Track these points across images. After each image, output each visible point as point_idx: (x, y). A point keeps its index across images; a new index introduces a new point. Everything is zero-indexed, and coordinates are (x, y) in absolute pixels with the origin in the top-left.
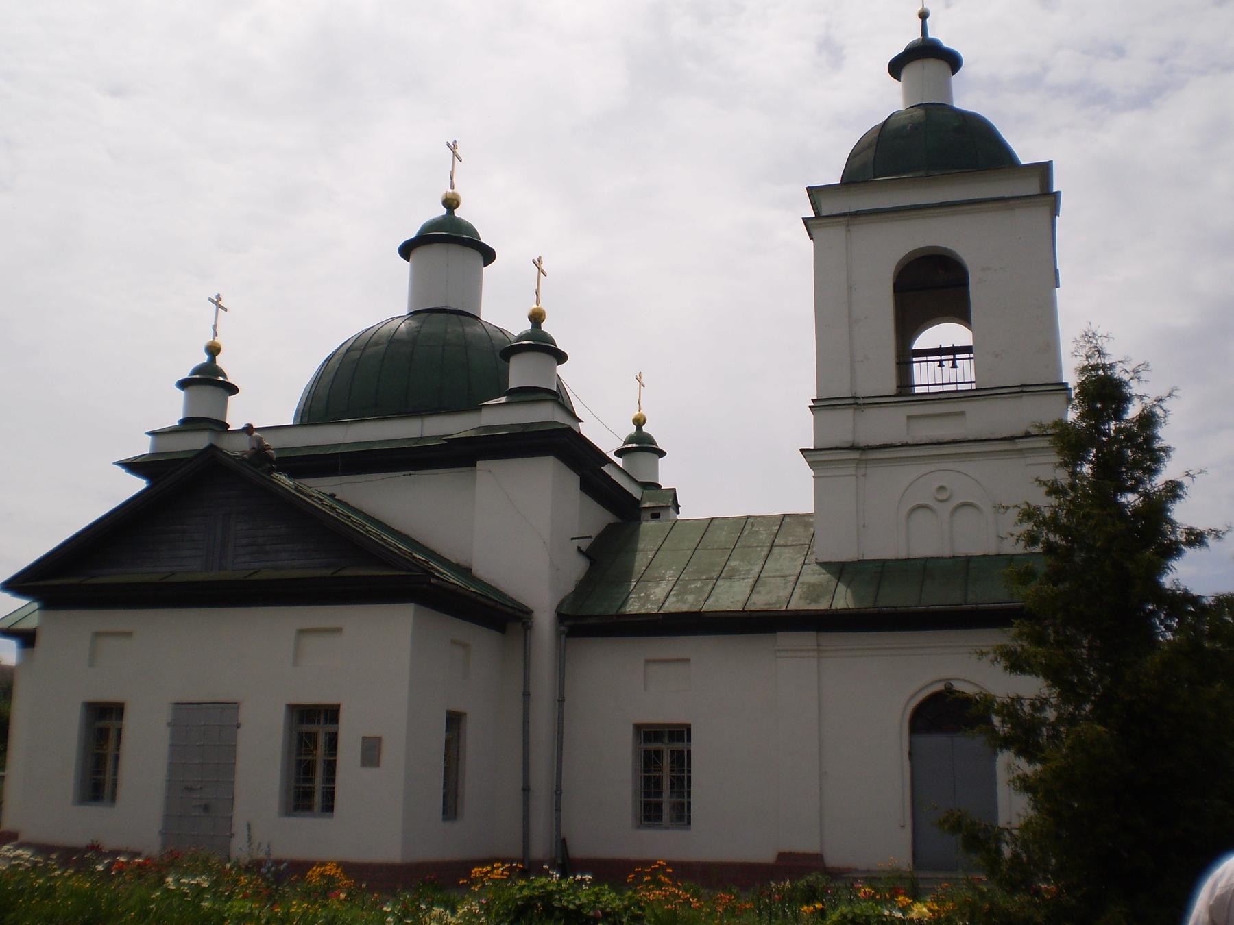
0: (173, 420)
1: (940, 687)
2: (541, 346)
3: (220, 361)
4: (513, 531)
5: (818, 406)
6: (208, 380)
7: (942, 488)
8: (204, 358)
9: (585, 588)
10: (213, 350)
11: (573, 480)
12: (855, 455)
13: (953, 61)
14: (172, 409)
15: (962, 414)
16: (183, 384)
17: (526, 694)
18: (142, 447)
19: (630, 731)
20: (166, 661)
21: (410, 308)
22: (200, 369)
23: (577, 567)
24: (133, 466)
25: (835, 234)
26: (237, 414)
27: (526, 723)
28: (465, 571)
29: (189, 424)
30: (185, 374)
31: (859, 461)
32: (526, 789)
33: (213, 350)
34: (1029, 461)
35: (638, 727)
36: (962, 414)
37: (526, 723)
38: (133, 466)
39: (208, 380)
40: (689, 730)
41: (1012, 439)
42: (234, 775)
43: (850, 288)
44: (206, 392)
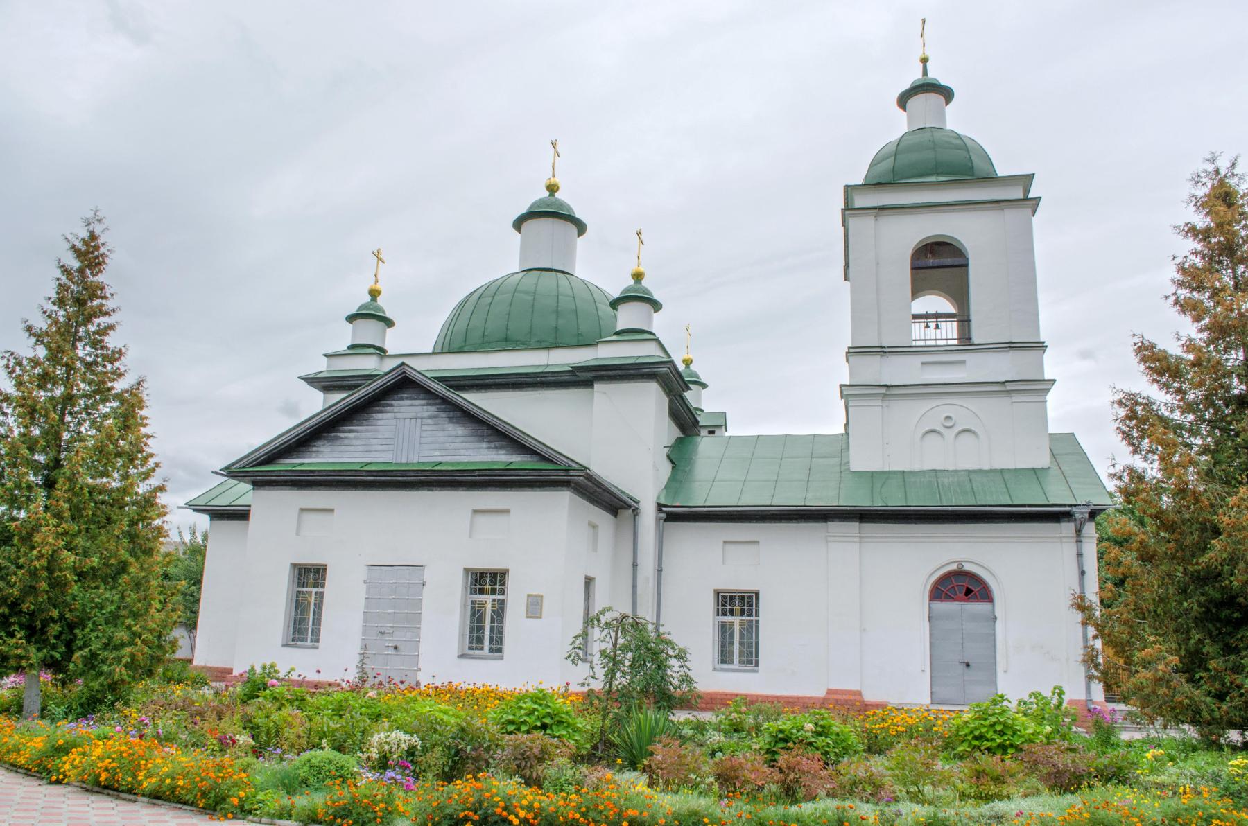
0: (343, 347)
1: (954, 567)
2: (638, 296)
5: (853, 352)
7: (948, 418)
12: (883, 391)
13: (947, 94)
14: (344, 336)
15: (963, 362)
16: (351, 318)
17: (635, 565)
20: (356, 536)
24: (312, 381)
26: (394, 342)
29: (357, 348)
30: (354, 311)
31: (885, 395)
34: (1014, 399)
35: (717, 593)
36: (963, 362)
38: (312, 381)
40: (757, 595)
41: (1003, 383)
42: (419, 622)
43: (878, 264)
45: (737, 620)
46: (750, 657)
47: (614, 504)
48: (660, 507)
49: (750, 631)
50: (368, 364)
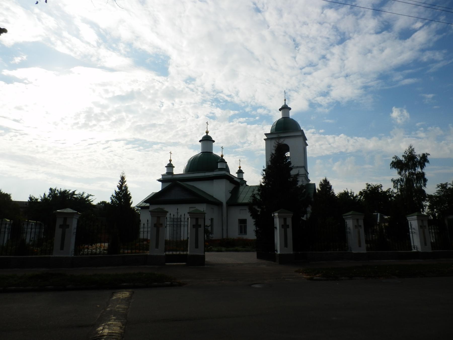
3: (172, 162)
4: (219, 190)
6: (170, 166)
8: (169, 162)
9: (231, 198)
10: (170, 161)
11: (229, 182)
14: (165, 171)
17: (222, 215)
18: (160, 177)
19: (237, 221)
21: (202, 150)
22: (168, 164)
23: (230, 195)
24: (159, 180)
25: (269, 141)
27: (222, 220)
28: (212, 197)
29: (168, 173)
32: (223, 229)
33: (170, 161)
35: (239, 220)
37: (222, 220)
38: (159, 180)
39: (170, 166)
44: (170, 168)
45: (243, 225)
46: (245, 233)
47: (218, 204)
48: (227, 203)
49: (245, 227)
50: (170, 176)
